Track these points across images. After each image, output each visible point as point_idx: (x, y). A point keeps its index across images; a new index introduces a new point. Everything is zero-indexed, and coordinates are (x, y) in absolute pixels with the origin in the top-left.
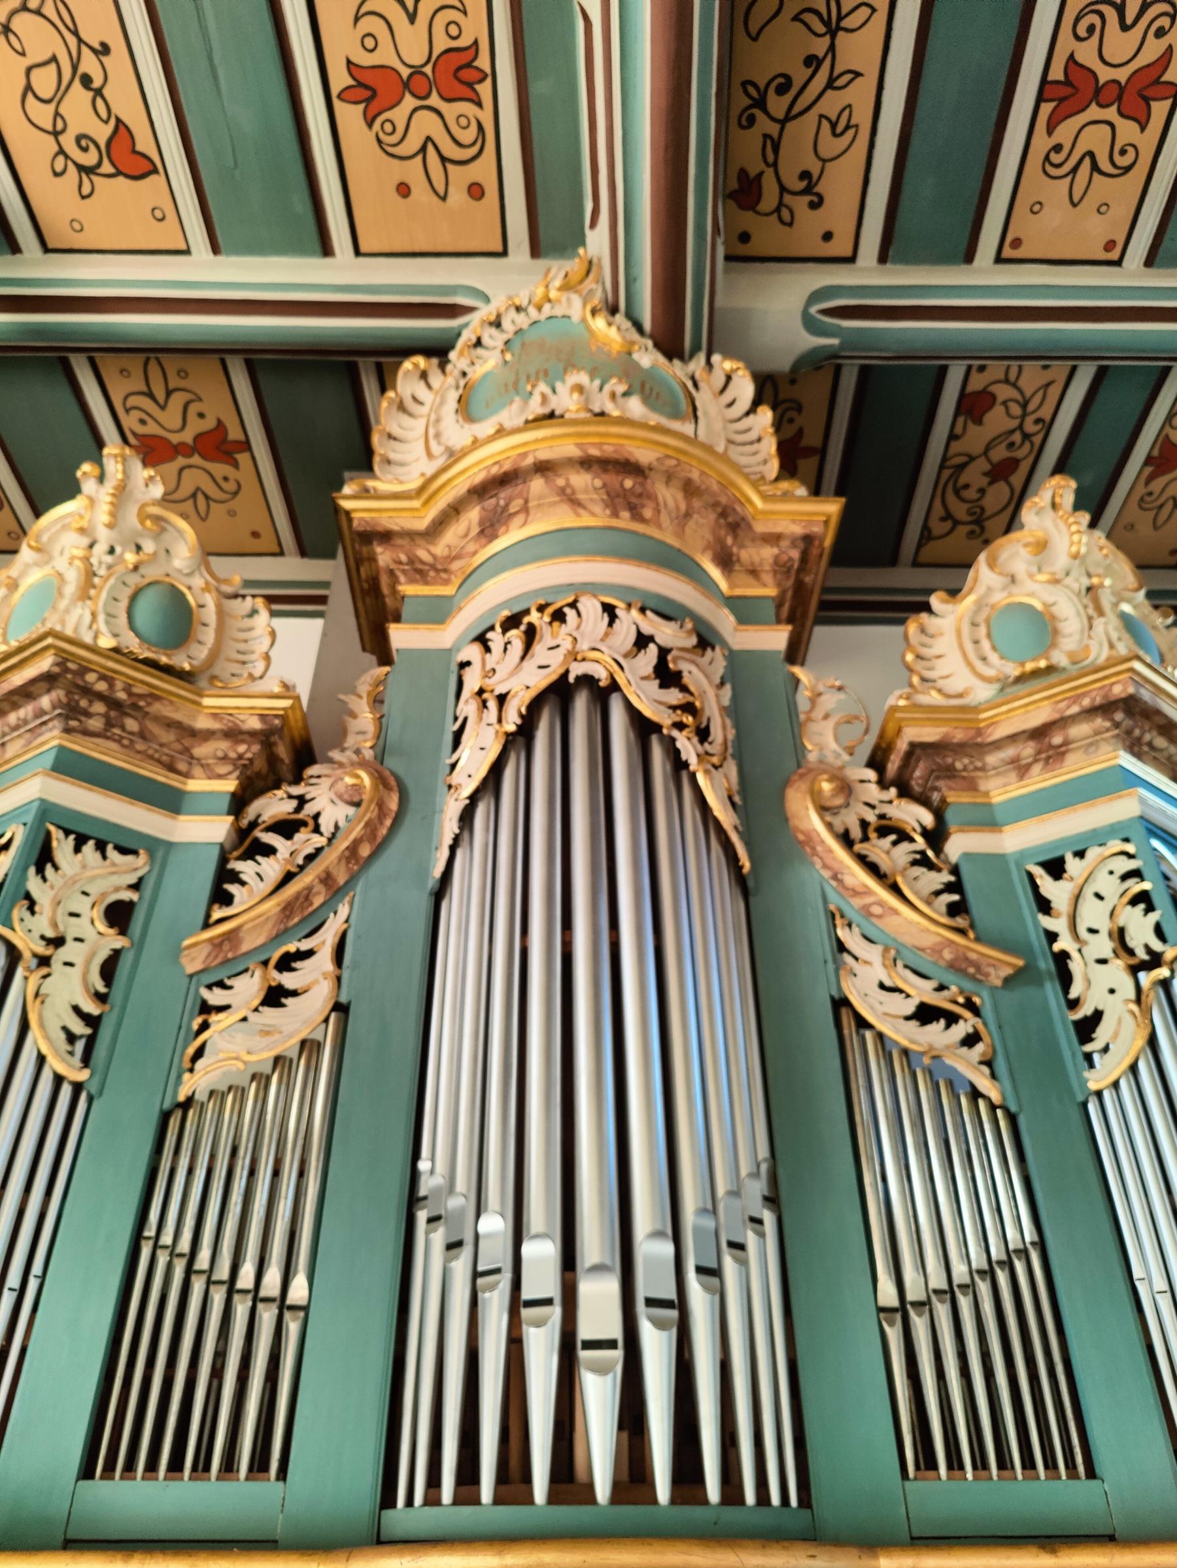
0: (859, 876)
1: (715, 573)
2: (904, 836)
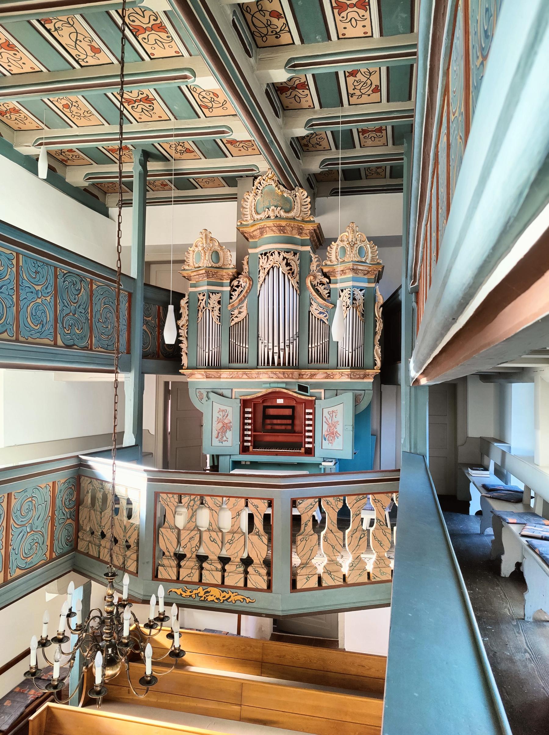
0: (314, 293)
1: (298, 237)
2: (323, 284)
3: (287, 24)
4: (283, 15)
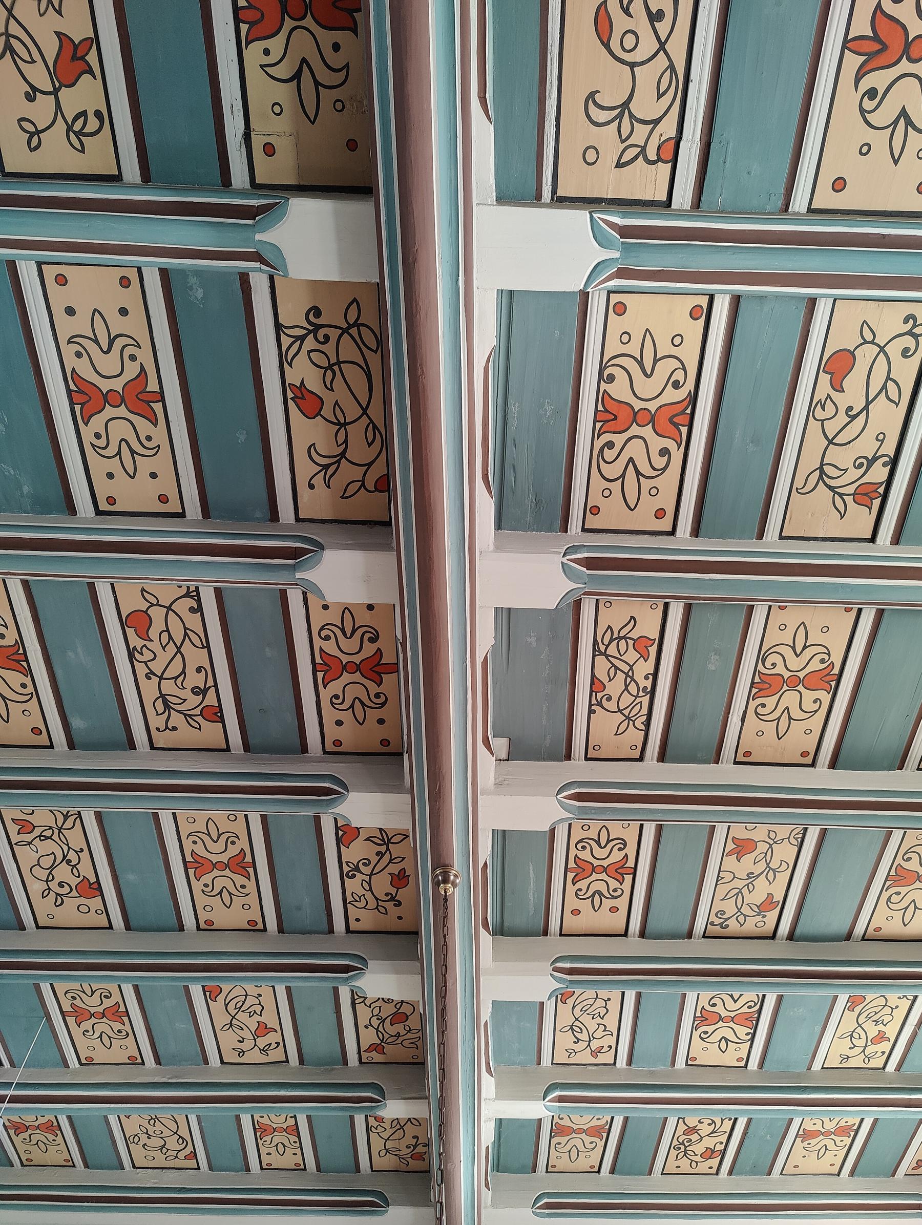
3: (283, 361)
4: (290, 395)
